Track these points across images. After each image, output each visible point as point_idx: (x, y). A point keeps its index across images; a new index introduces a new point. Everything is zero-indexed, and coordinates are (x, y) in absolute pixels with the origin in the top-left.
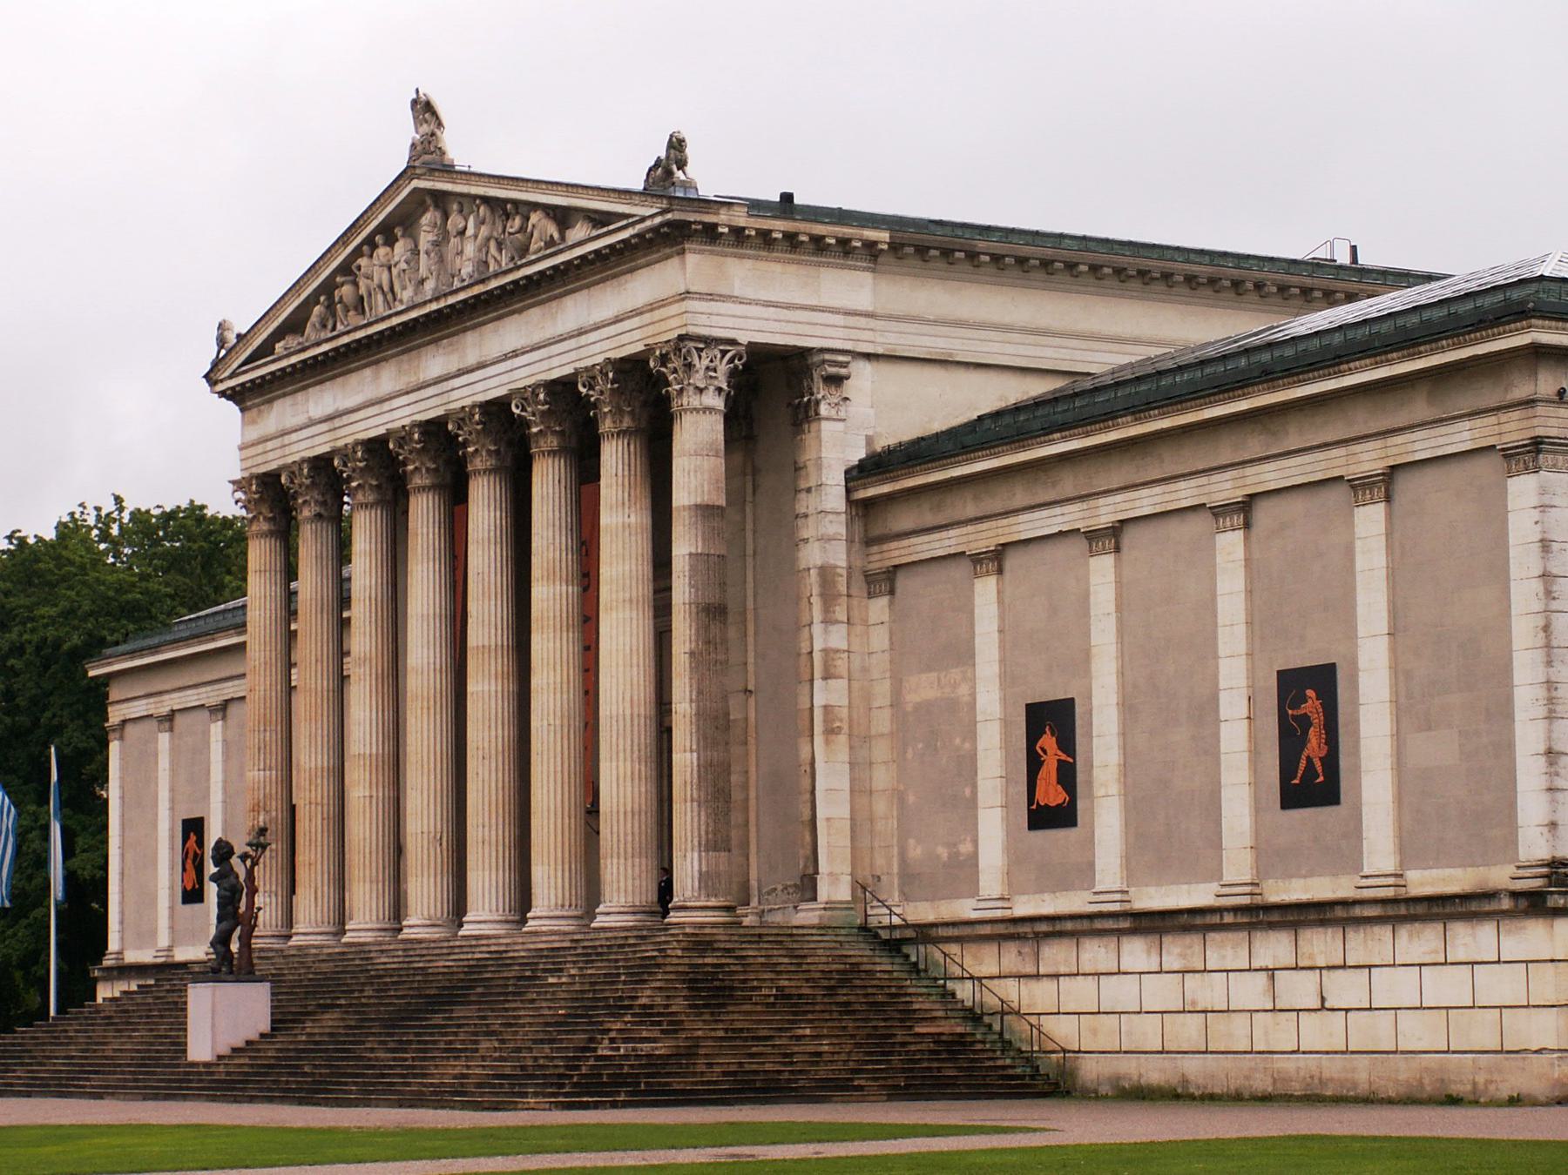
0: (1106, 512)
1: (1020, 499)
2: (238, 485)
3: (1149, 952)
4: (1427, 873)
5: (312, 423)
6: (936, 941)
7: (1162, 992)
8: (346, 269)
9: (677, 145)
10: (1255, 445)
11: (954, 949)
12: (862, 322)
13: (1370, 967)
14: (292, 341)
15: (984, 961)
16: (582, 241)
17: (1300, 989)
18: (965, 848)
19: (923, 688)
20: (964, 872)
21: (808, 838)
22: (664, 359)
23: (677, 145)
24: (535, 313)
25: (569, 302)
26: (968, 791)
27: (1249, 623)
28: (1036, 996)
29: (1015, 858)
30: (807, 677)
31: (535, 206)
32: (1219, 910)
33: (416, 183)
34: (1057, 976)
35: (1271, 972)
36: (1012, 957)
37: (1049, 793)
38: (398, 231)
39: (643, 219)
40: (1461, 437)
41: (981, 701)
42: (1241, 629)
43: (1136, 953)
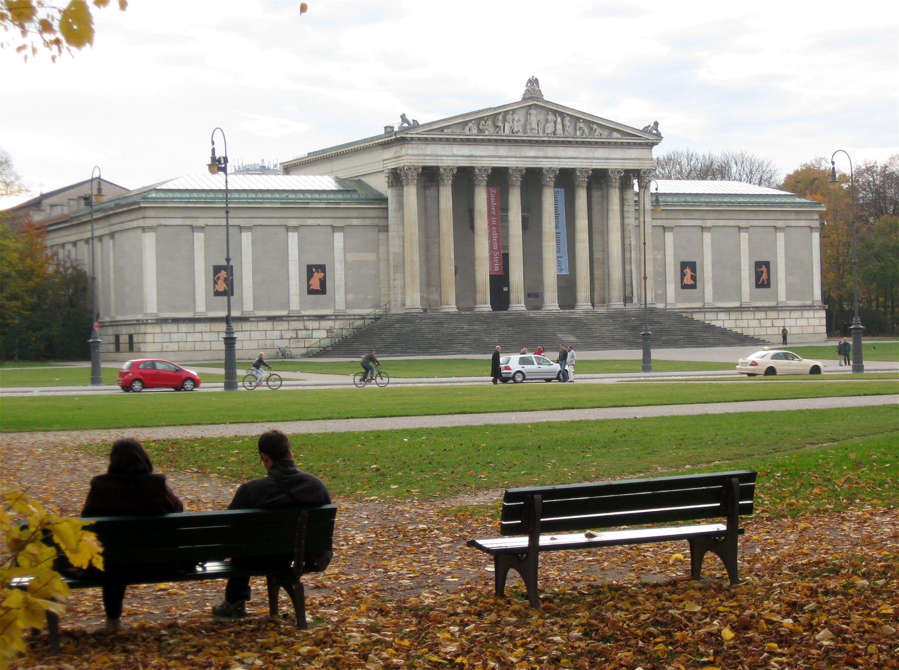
0: (709, 223)
9: (656, 124)
10: (751, 216)
16: (604, 136)
22: (644, 173)
23: (656, 124)
25: (600, 150)
35: (760, 320)
37: (688, 280)
40: (803, 223)
43: (722, 316)
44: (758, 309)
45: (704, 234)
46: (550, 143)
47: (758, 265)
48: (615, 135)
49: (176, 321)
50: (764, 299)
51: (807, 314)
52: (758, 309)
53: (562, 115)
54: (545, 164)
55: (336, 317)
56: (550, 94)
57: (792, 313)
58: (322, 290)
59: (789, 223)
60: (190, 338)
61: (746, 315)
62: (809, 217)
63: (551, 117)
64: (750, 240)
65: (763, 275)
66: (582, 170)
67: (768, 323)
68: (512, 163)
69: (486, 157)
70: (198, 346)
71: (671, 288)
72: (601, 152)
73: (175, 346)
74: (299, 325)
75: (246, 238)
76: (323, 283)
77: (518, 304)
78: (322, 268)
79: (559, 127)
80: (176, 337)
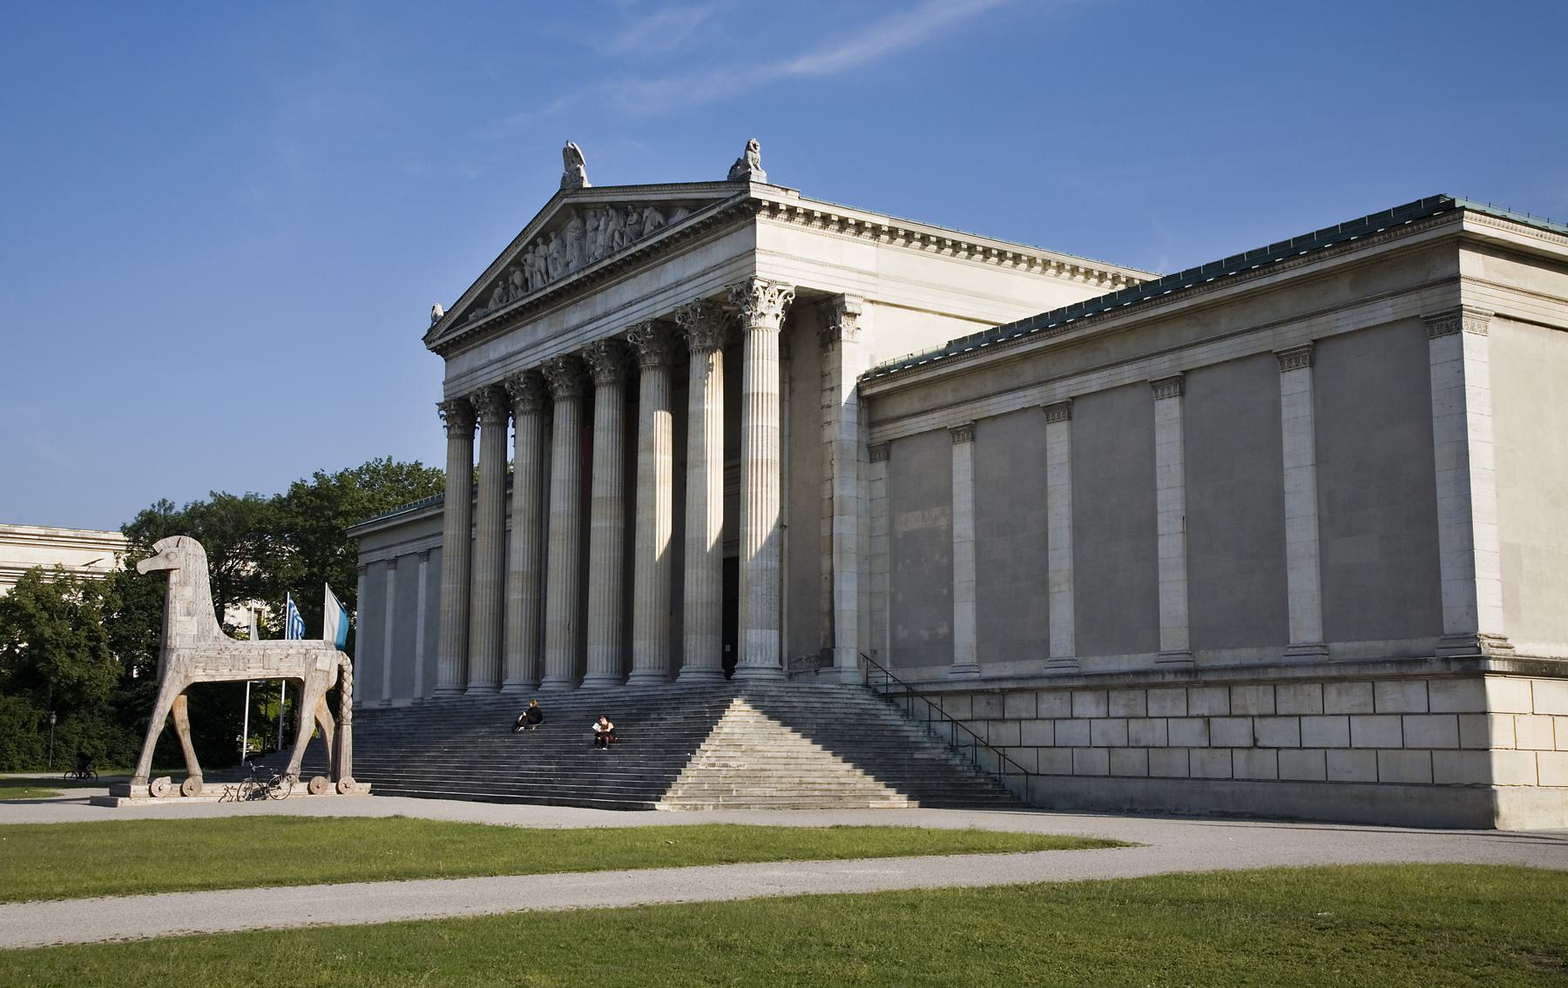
0: (1061, 391)
1: (990, 387)
2: (442, 406)
3: (1098, 705)
4: (1349, 645)
5: (491, 363)
6: (922, 695)
7: (1114, 732)
8: (518, 263)
10: (1188, 333)
11: (935, 700)
12: (871, 279)
13: (1300, 716)
14: (480, 312)
15: (962, 710)
16: (684, 222)
17: (1237, 732)
18: (943, 630)
19: (913, 522)
20: (944, 647)
21: (827, 624)
24: (645, 276)
25: (669, 266)
26: (945, 591)
27: (1185, 464)
30: (827, 513)
31: (646, 204)
32: (1162, 672)
33: (565, 201)
34: (1019, 720)
35: (1207, 719)
36: (981, 707)
38: (552, 235)
39: (727, 200)
40: (1385, 311)
41: (957, 528)
42: (1177, 469)
43: (1086, 705)
45: (1049, 428)
51: (1392, 696)
57: (1332, 690)
62: (1411, 277)
64: (1187, 424)
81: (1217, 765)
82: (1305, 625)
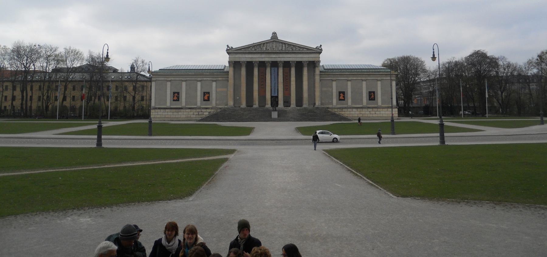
0: (350, 78)
9: (321, 46)
15: (336, 110)
18: (330, 101)
20: (332, 103)
23: (321, 46)
28: (343, 113)
29: (337, 104)
36: (339, 110)
37: (342, 98)
43: (354, 110)
44: (369, 108)
46: (280, 53)
47: (370, 92)
48: (305, 50)
49: (159, 108)
50: (372, 104)
52: (369, 108)
53: (285, 44)
54: (278, 60)
55: (212, 108)
56: (280, 38)
58: (208, 100)
59: (382, 78)
60: (164, 114)
61: (364, 110)
63: (281, 45)
65: (372, 96)
66: (292, 61)
67: (374, 113)
68: (266, 60)
69: (257, 58)
70: (166, 116)
71: (335, 101)
72: (300, 56)
73: (159, 116)
74: (200, 110)
75: (184, 84)
76: (209, 97)
77: (256, 105)
78: (209, 93)
79: (284, 48)
80: (159, 113)
81: (371, 115)
82: (380, 103)
